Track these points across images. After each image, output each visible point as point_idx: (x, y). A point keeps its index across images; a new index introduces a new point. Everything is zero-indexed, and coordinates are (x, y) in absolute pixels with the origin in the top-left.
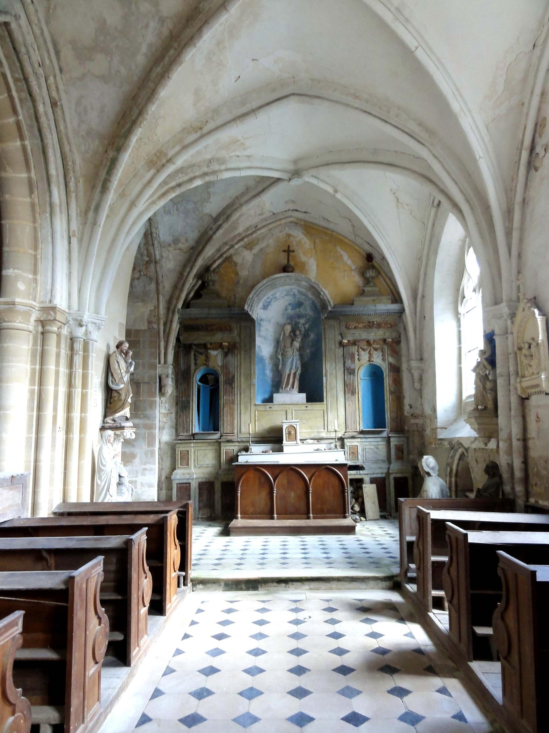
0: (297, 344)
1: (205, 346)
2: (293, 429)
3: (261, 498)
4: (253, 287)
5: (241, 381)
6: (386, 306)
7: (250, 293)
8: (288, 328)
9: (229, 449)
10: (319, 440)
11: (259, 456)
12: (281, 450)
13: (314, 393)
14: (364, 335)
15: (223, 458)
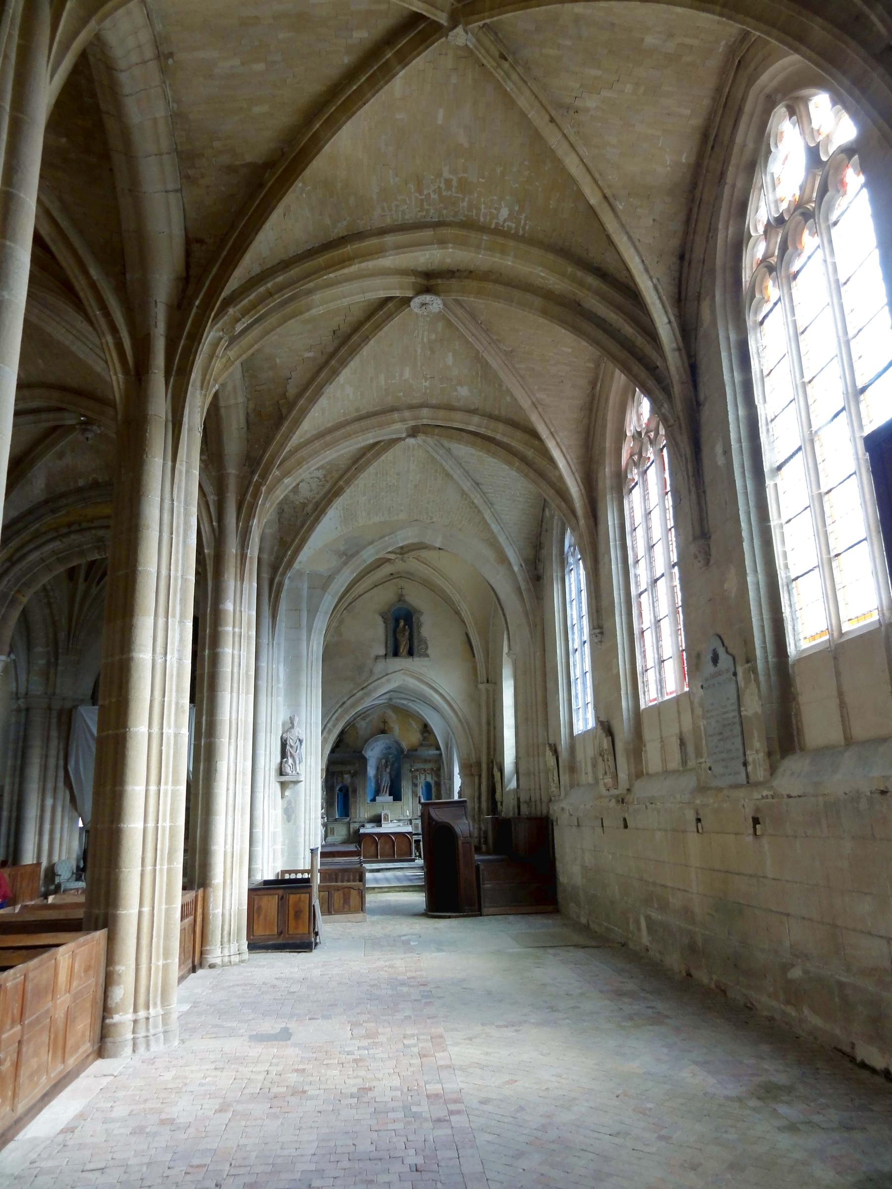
0: (388, 770)
2: (386, 815)
4: (367, 740)
5: (360, 791)
6: (433, 752)
7: (365, 743)
8: (384, 761)
9: (354, 826)
10: (399, 820)
11: (369, 829)
14: (422, 766)
15: (352, 830)
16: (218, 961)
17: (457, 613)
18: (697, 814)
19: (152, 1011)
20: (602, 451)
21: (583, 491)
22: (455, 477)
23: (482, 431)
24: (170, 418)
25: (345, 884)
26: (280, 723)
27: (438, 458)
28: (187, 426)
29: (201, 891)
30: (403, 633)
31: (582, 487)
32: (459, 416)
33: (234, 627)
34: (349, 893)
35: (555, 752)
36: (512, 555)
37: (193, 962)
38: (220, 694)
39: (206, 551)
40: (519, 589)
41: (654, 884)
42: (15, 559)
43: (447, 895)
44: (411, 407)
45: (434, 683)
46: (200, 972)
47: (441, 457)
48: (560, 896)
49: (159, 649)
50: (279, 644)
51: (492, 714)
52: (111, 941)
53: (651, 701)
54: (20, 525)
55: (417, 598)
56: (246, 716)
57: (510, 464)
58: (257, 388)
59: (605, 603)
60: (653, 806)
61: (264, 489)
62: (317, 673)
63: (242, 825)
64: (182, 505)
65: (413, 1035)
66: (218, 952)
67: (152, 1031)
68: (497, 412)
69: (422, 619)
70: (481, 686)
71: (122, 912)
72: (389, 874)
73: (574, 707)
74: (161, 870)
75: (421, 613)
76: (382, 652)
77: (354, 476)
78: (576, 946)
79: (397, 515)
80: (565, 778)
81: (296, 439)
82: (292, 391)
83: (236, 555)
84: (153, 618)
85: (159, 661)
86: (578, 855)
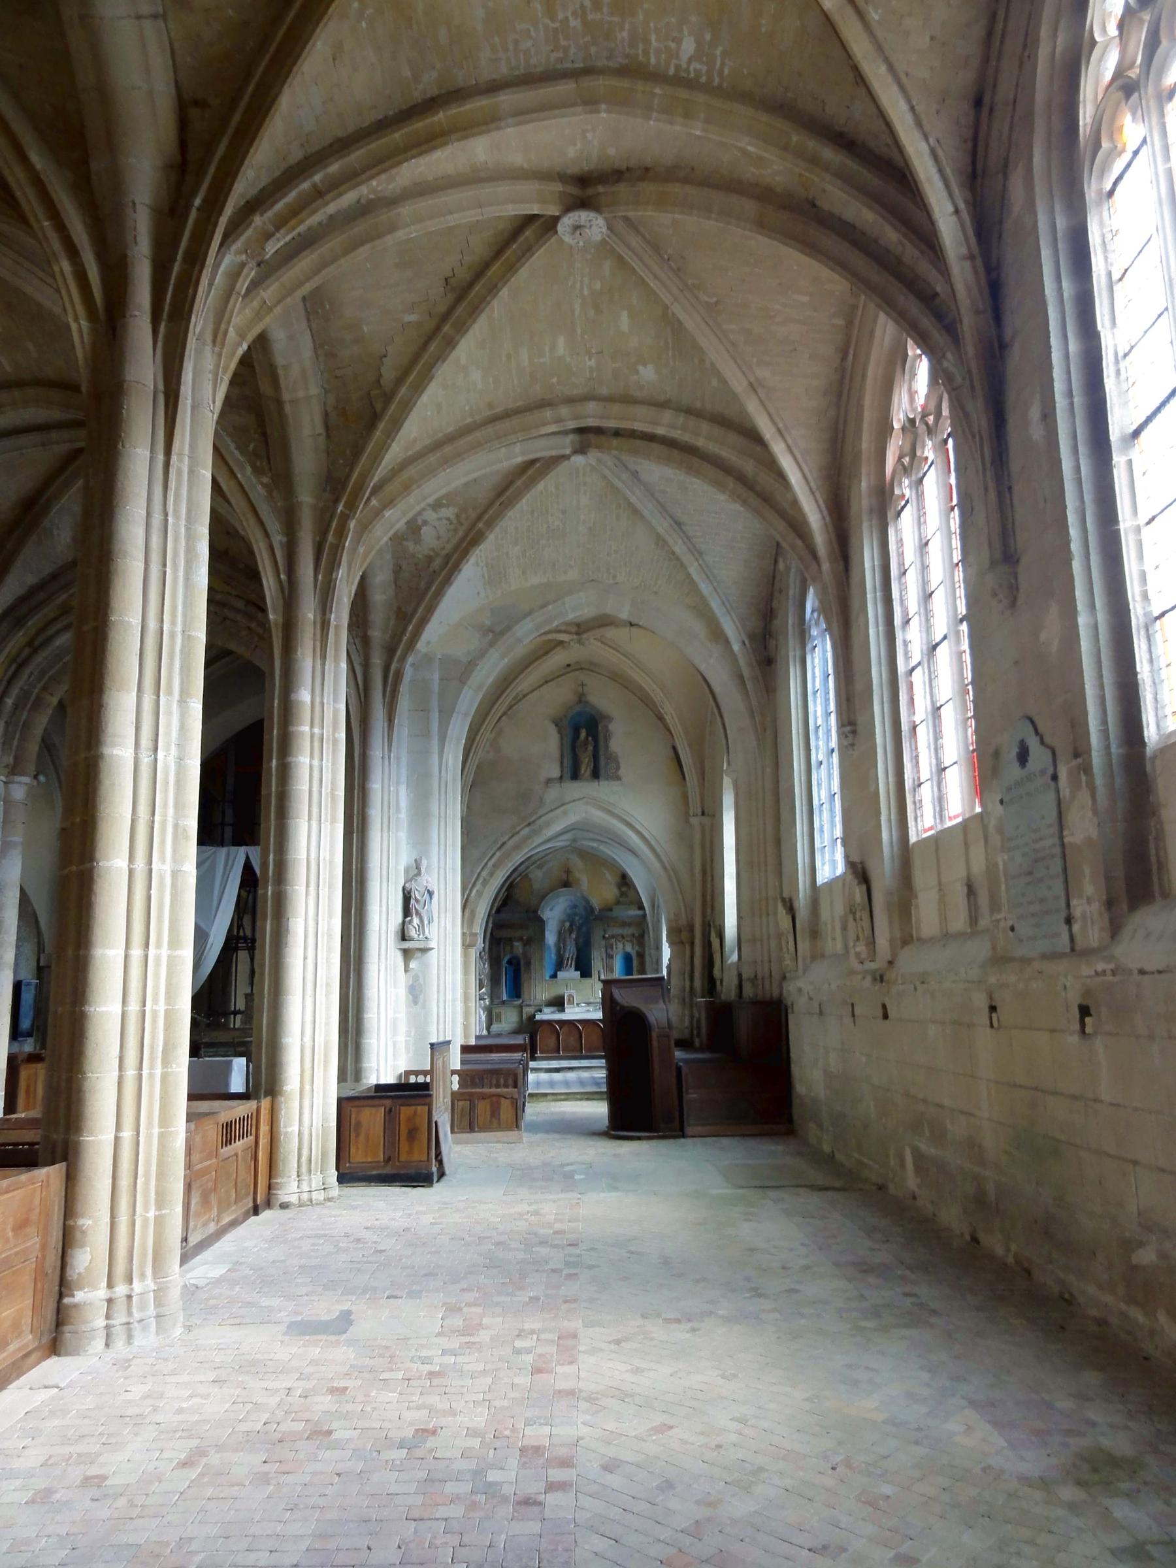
0: (574, 936)
1: (511, 940)
2: (571, 996)
3: (552, 1042)
4: (543, 898)
5: (535, 965)
6: (634, 912)
8: (567, 924)
9: (528, 1011)
10: (588, 1004)
11: (548, 1014)
12: (563, 1010)
13: (586, 973)
15: (524, 1016)
16: (293, 1199)
17: (660, 718)
18: (991, 998)
19: (137, 1286)
20: (857, 455)
21: (828, 519)
22: (646, 513)
23: (676, 434)
24: (161, 387)
25: (494, 1090)
26: (402, 868)
27: (619, 485)
28: (189, 402)
29: (265, 1103)
30: (585, 745)
31: (826, 513)
32: (641, 411)
33: (312, 726)
34: (499, 1103)
35: (791, 909)
36: (730, 628)
37: (255, 1200)
38: (291, 823)
39: (271, 617)
40: (741, 677)
41: (925, 1101)
42: (37, 643)
43: (639, 1108)
44: (571, 401)
45: (630, 816)
46: (266, 1215)
47: (624, 482)
48: (796, 1111)
49: (146, 742)
50: (398, 758)
51: (708, 859)
52: (71, 1180)
53: (926, 831)
54: (41, 596)
55: (603, 698)
56: (332, 854)
57: (720, 486)
58: (338, 373)
59: (859, 686)
60: (925, 986)
61: (352, 524)
62: (455, 798)
63: (328, 1008)
64: (183, 522)
65: (533, 1332)
66: (293, 1186)
67: (137, 1315)
68: (698, 405)
69: (612, 727)
70: (695, 821)
71: (87, 1138)
72: (571, 1075)
73: (817, 844)
74: (151, 1076)
75: (609, 718)
76: (555, 772)
77: (500, 515)
78: (813, 1187)
79: (565, 573)
80: (804, 946)
81: (396, 452)
82: (388, 374)
83: (315, 622)
84: (134, 694)
85: (146, 760)
86: (819, 1056)
